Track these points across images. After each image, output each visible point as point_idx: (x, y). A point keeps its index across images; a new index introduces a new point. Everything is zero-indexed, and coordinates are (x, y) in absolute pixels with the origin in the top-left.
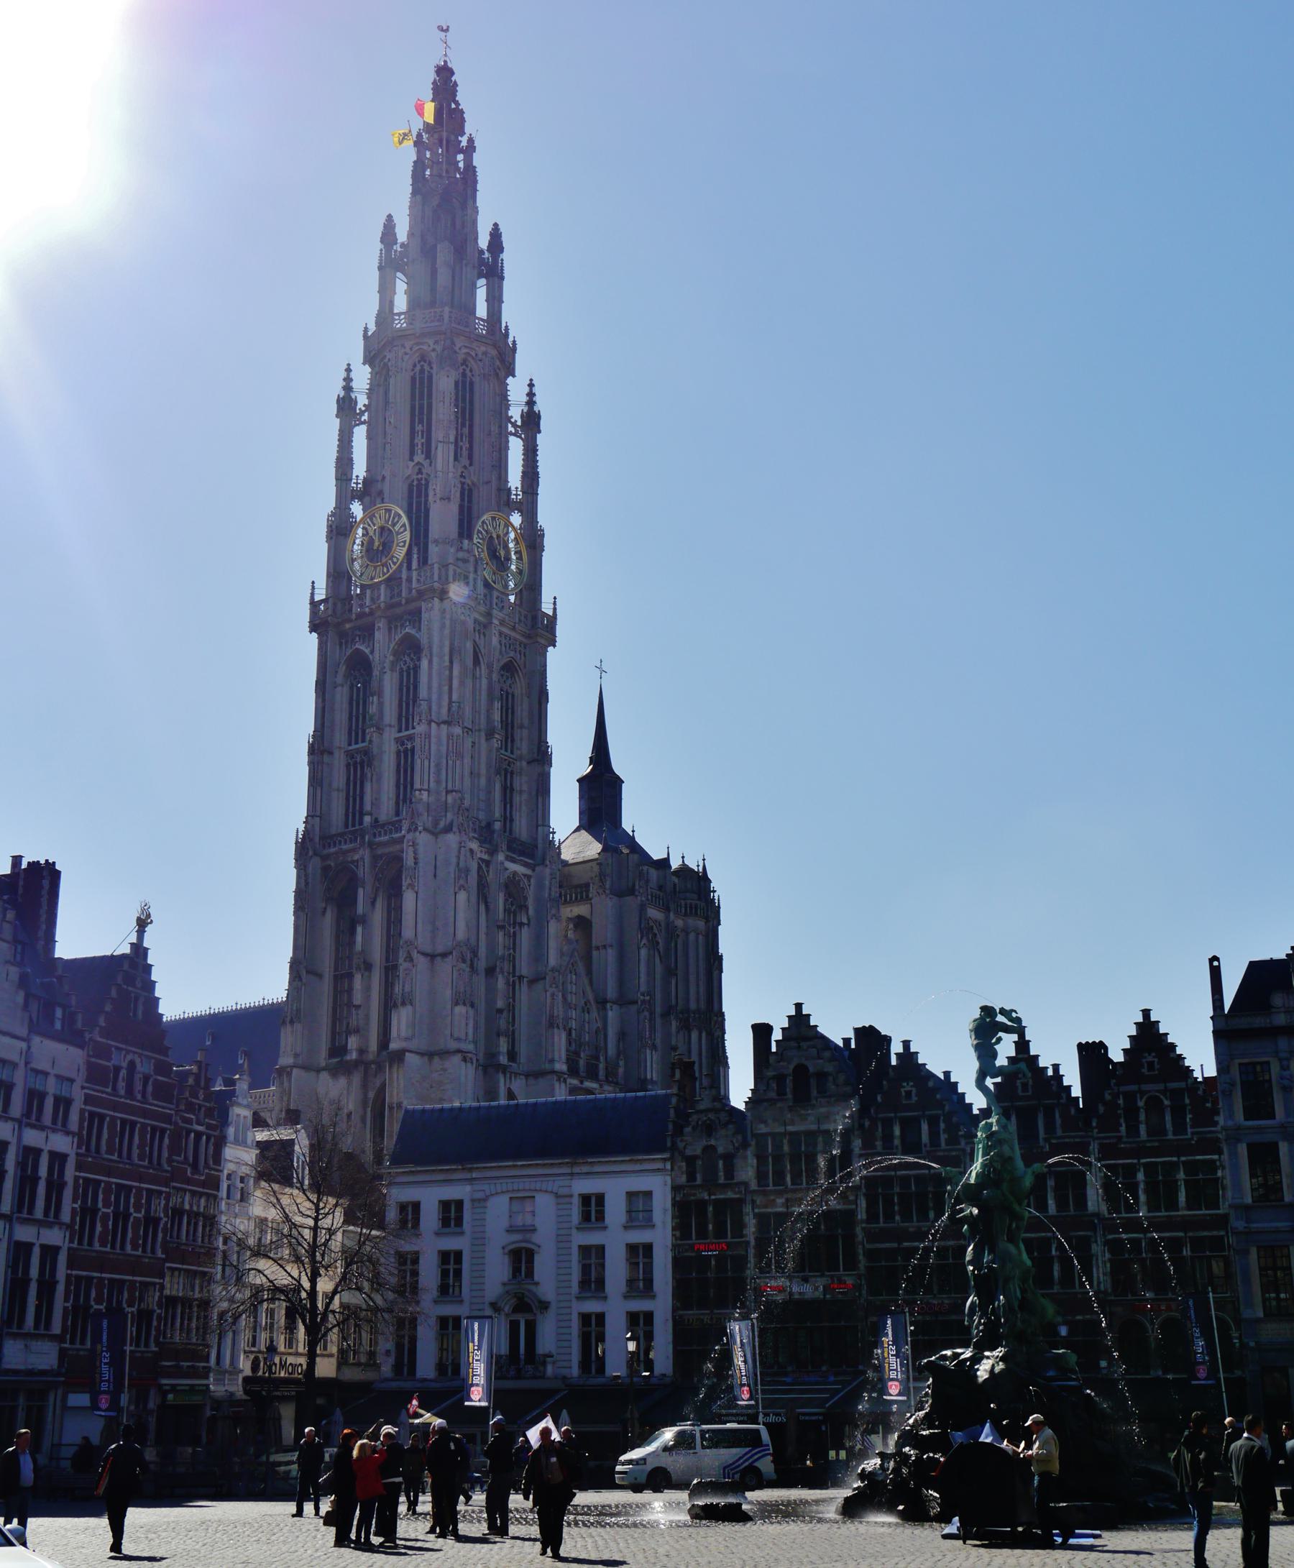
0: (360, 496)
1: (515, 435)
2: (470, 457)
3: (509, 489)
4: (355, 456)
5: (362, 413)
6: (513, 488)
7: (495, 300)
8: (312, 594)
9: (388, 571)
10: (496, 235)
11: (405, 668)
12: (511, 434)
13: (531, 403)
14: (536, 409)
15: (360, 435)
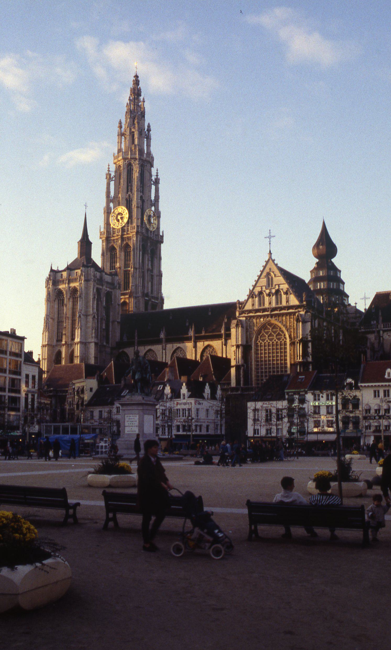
0: (112, 201)
1: (153, 184)
2: (143, 193)
3: (152, 200)
4: (111, 190)
5: (113, 178)
6: (153, 200)
7: (149, 145)
8: (100, 229)
9: (122, 225)
10: (149, 126)
11: (126, 251)
12: (152, 184)
13: (157, 175)
14: (159, 177)
15: (112, 183)
